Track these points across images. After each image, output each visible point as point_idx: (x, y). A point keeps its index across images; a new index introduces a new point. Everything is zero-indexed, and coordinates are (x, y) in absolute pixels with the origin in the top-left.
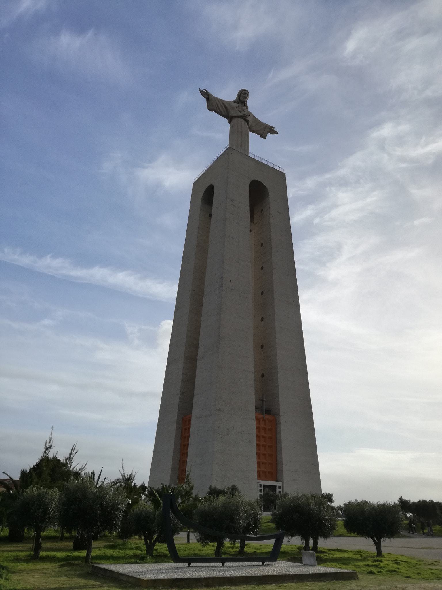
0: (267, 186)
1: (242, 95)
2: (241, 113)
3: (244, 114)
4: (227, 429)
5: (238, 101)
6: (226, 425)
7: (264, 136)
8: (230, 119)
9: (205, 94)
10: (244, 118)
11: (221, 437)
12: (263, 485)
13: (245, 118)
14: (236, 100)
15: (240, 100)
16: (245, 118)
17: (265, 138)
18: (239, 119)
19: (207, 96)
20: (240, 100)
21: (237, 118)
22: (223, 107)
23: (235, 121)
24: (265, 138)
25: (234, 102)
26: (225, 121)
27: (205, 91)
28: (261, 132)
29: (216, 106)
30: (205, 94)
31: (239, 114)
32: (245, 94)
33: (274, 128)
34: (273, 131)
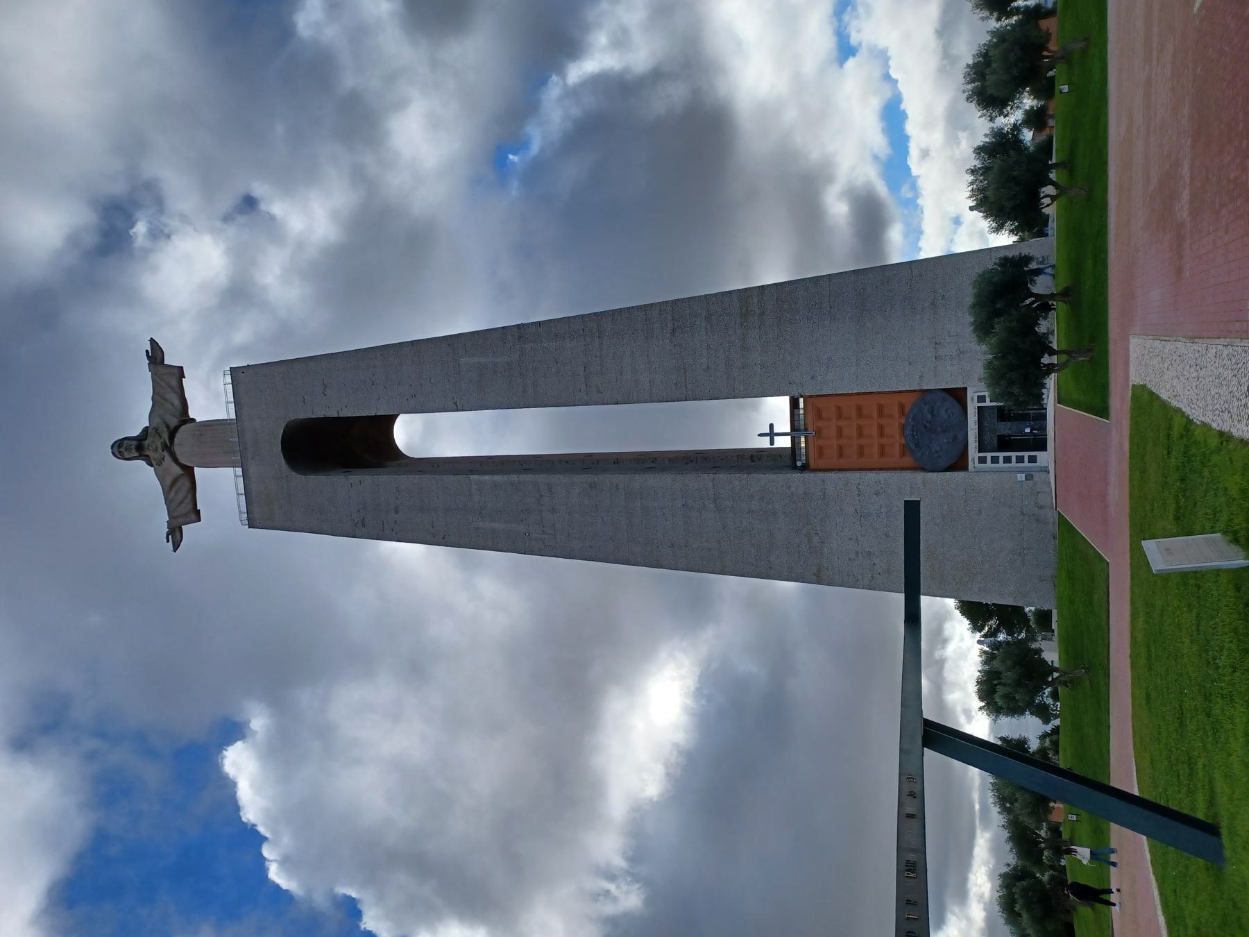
0: (283, 425)
1: (127, 457)
4: (858, 556)
5: (141, 458)
6: (850, 560)
7: (180, 372)
8: (189, 472)
9: (175, 535)
11: (879, 574)
12: (979, 452)
15: (141, 455)
22: (174, 489)
27: (170, 536)
28: (174, 382)
29: (183, 505)
30: (175, 535)
33: (147, 351)
34: (155, 355)
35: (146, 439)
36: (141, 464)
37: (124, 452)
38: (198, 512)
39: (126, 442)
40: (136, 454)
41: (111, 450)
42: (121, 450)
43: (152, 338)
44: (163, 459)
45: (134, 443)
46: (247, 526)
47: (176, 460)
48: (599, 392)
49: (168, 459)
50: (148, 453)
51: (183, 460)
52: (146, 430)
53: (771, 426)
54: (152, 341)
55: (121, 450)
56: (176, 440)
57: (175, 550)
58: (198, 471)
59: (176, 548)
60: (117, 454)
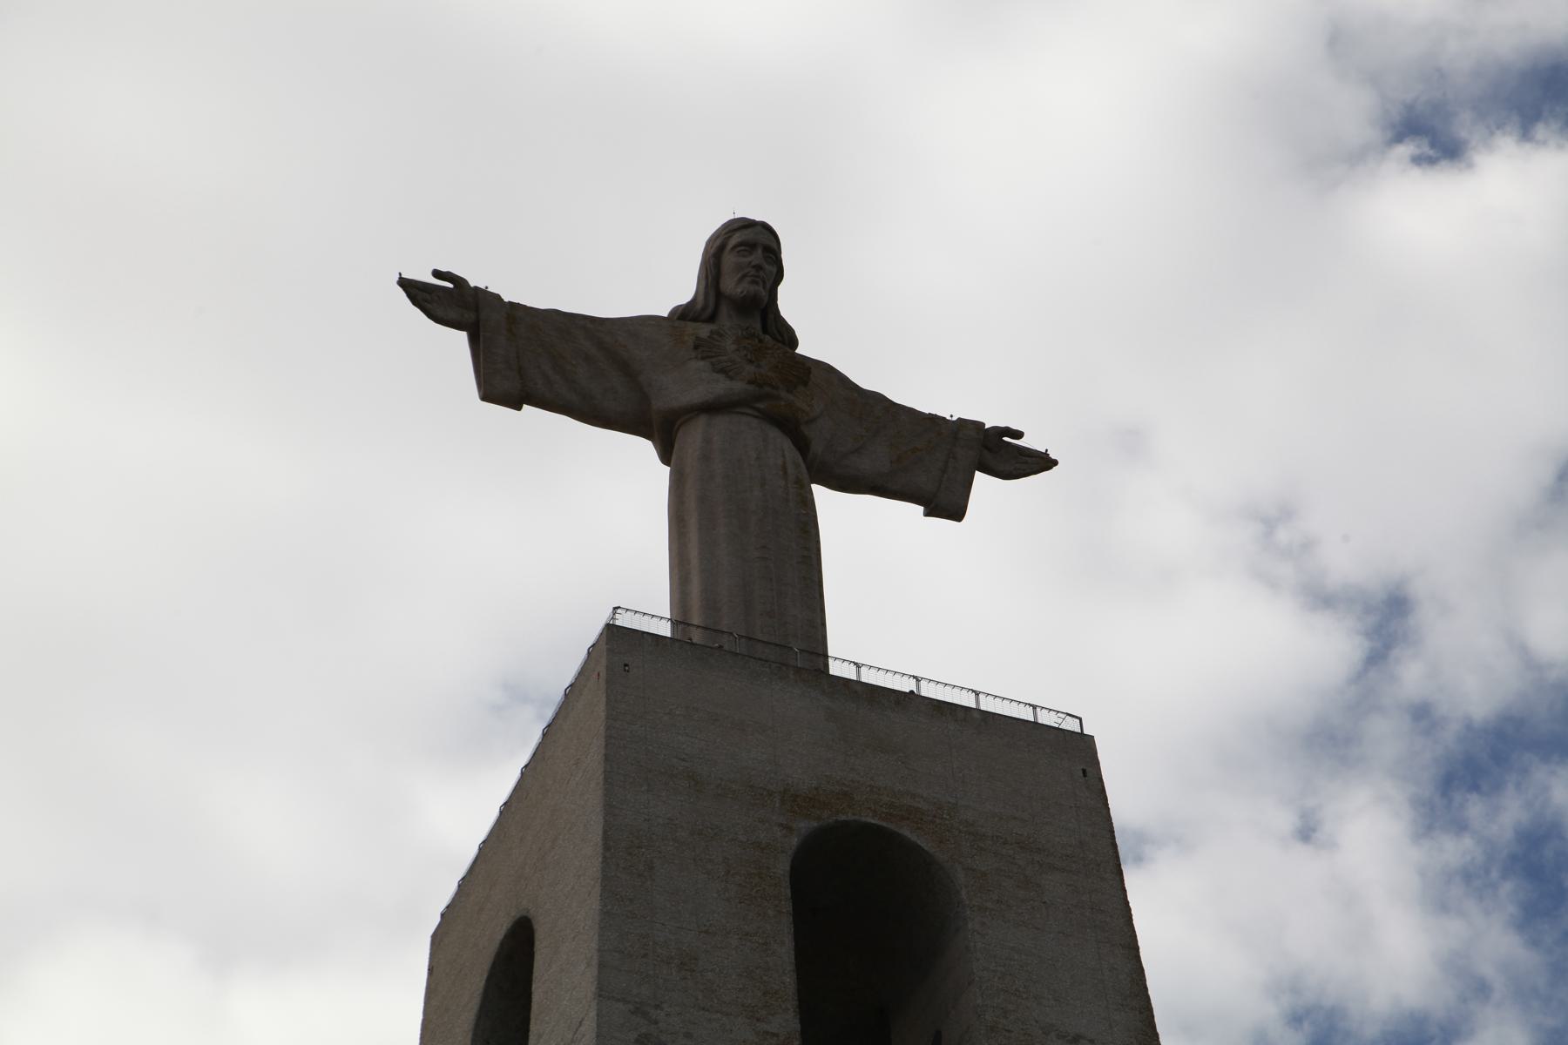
1: (729, 260)
2: (731, 379)
3: (750, 382)
10: (758, 410)
13: (761, 406)
14: (693, 301)
15: (719, 294)
16: (761, 406)
17: (955, 512)
18: (722, 423)
19: (470, 316)
20: (719, 294)
21: (702, 420)
23: (692, 437)
24: (955, 512)
26: (641, 450)
27: (450, 285)
32: (749, 246)
33: (1019, 435)
38: (514, 401)
39: (774, 270)
40: (731, 285)
43: (1055, 463)
44: (722, 371)
45: (764, 294)
47: (711, 408)
49: (720, 387)
52: (788, 337)
55: (759, 251)
56: (774, 434)
57: (405, 284)
59: (414, 291)
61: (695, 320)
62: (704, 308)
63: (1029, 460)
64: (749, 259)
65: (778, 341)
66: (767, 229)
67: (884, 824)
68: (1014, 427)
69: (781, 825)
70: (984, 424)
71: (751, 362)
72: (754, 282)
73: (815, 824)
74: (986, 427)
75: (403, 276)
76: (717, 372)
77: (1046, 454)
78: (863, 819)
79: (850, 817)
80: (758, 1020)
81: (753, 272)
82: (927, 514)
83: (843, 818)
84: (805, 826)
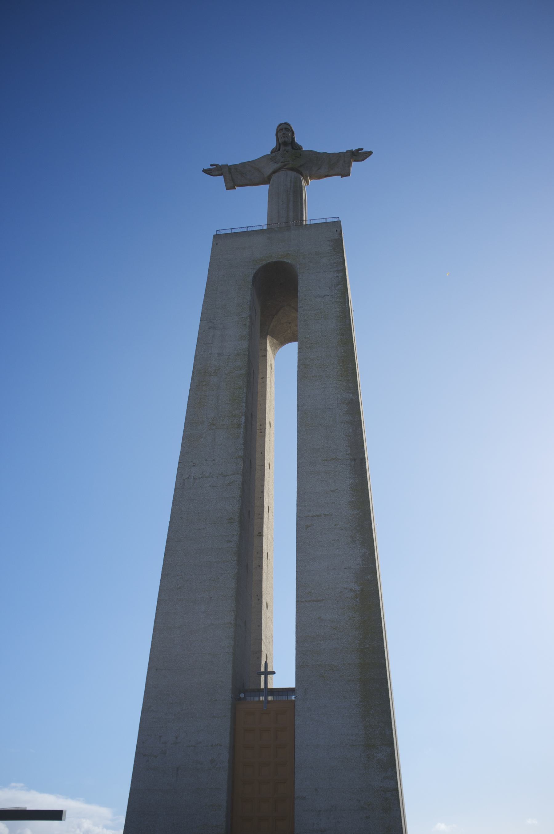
1: (279, 134)
2: (278, 163)
3: (281, 163)
6: (160, 737)
7: (346, 173)
10: (286, 168)
13: (286, 167)
14: (275, 148)
16: (286, 167)
17: (348, 175)
18: (276, 174)
20: (279, 143)
21: (274, 175)
23: (271, 181)
24: (348, 175)
25: (272, 152)
31: (276, 166)
33: (362, 149)
35: (293, 148)
36: (273, 144)
37: (282, 133)
41: (283, 122)
42: (284, 130)
43: (372, 153)
44: (276, 162)
46: (215, 234)
47: (274, 172)
48: (307, 527)
50: (281, 149)
51: (274, 178)
53: (273, 673)
54: (369, 153)
58: (264, 189)
59: (206, 171)
60: (281, 127)
61: (275, 152)
62: (276, 149)
63: (367, 154)
64: (281, 133)
65: (295, 149)
66: (286, 124)
67: (279, 260)
68: (360, 148)
69: (252, 268)
70: (353, 150)
71: (283, 157)
72: (284, 138)
73: (261, 265)
74: (354, 150)
75: (204, 169)
76: (275, 163)
77: (371, 151)
78: (274, 261)
79: (270, 261)
80: (239, 315)
81: (283, 135)
82: (341, 177)
83: (269, 262)
84: (257, 267)
